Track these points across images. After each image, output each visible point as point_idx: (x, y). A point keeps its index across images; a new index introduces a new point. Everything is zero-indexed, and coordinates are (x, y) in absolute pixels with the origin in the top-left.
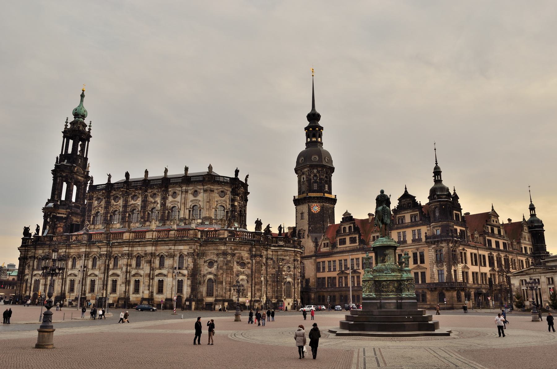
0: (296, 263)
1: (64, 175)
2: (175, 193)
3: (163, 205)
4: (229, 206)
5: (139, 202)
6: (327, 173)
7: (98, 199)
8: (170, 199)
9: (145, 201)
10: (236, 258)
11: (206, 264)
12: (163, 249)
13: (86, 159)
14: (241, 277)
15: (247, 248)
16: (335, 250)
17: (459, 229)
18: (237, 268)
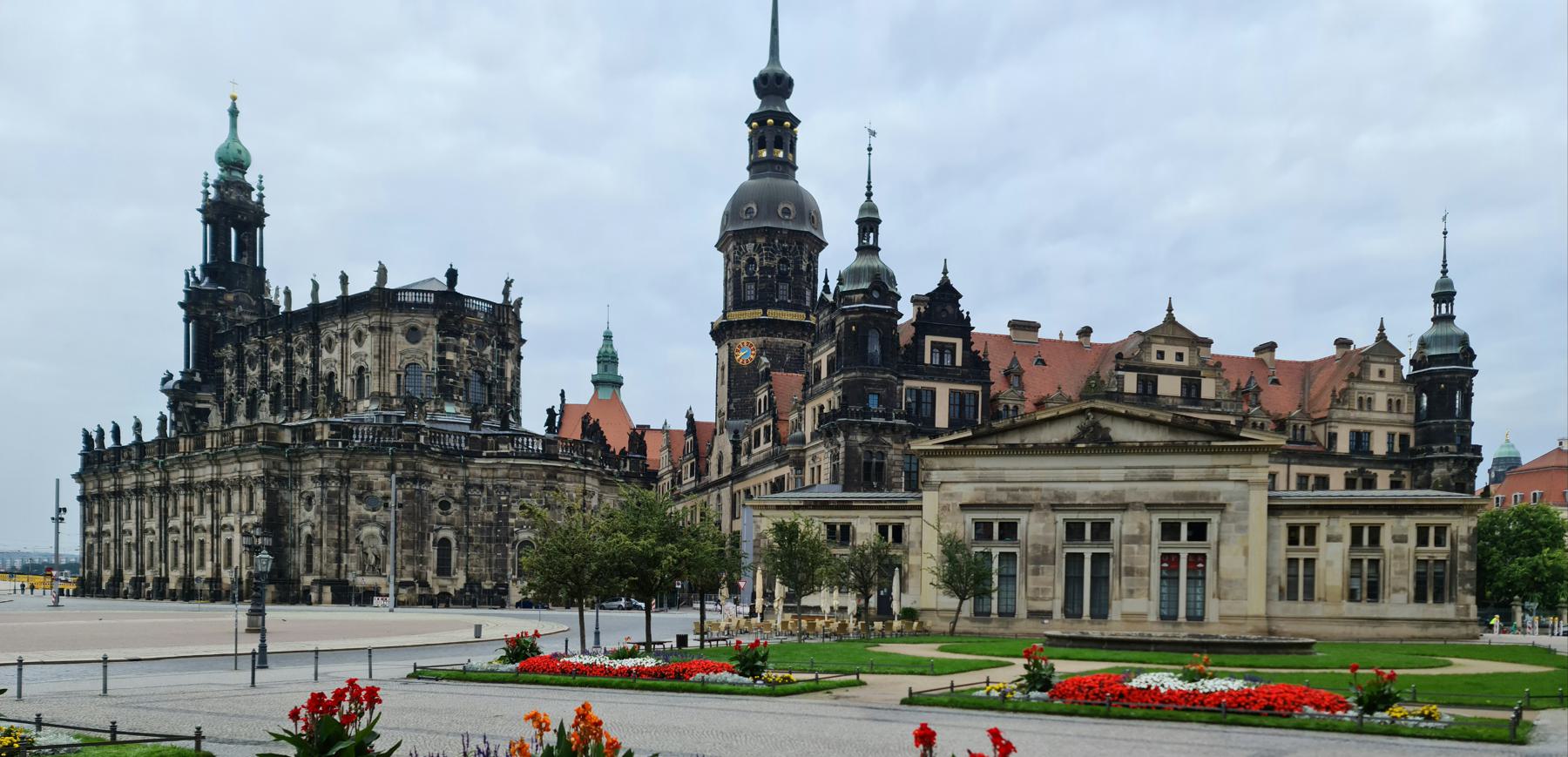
0: (552, 494)
1: (203, 313)
2: (330, 340)
3: (315, 369)
4: (433, 365)
5: (278, 368)
6: (784, 251)
7: (230, 365)
8: (325, 354)
9: (289, 365)
10: (353, 488)
11: (303, 502)
12: (230, 471)
13: (262, 271)
14: (367, 530)
15: (386, 461)
16: (752, 462)
17: (943, 391)
18: (356, 509)
